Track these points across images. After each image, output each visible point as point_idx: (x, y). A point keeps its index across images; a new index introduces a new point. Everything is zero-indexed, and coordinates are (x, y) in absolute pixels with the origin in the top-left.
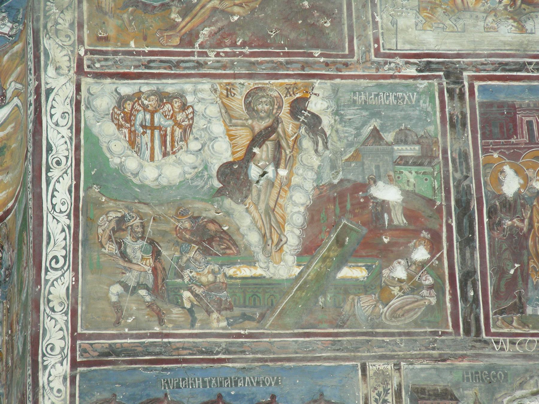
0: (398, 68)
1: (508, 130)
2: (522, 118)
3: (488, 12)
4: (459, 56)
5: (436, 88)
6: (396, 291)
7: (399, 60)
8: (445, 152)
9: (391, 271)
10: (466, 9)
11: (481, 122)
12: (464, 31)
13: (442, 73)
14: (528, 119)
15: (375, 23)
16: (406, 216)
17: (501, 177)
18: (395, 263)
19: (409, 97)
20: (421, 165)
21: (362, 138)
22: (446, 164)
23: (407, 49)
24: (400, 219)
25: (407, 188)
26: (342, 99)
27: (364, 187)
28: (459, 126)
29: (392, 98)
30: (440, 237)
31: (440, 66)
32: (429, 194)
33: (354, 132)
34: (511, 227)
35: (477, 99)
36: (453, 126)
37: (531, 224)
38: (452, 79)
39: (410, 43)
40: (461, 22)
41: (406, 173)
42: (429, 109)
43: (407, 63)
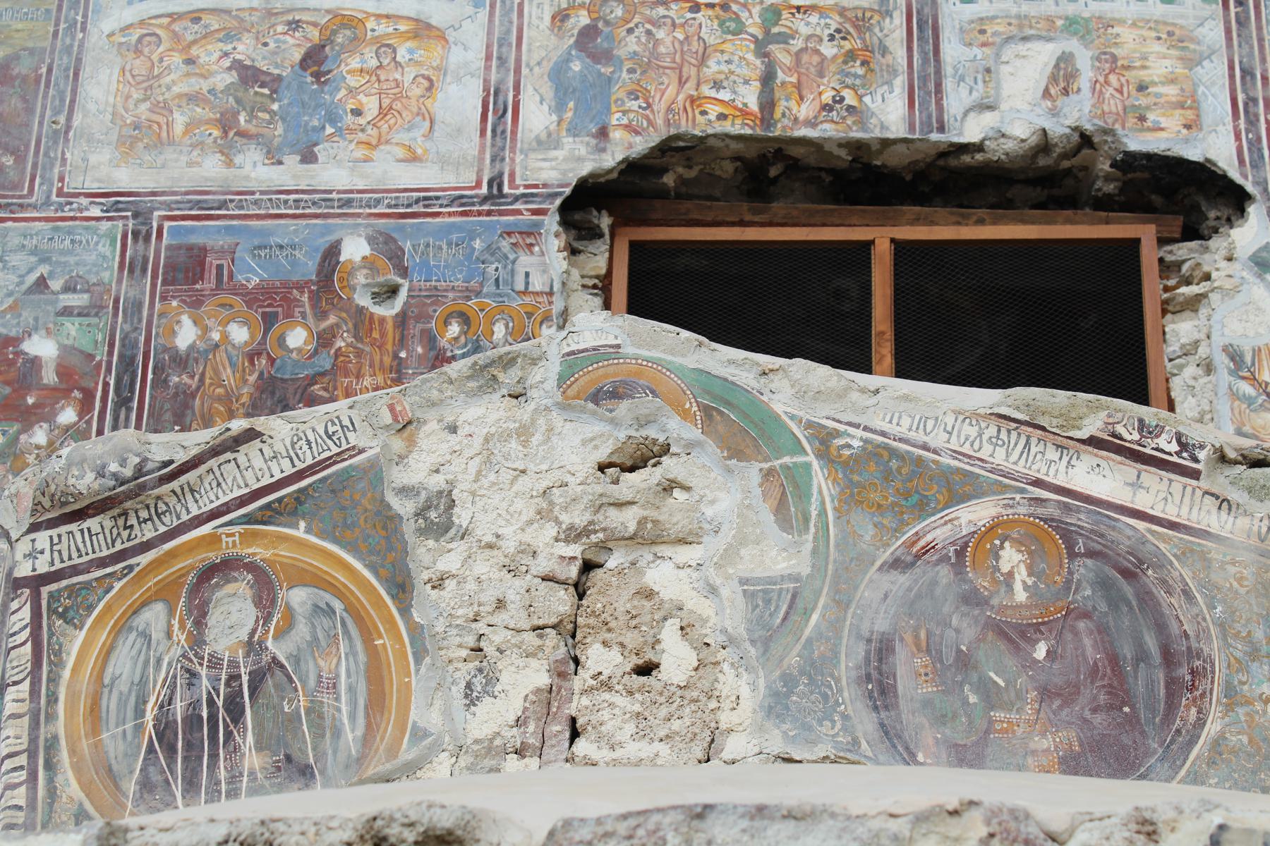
0: (81, 211)
1: (194, 275)
2: (212, 261)
3: (193, 146)
4: (154, 194)
5: (120, 230)
6: (31, 459)
7: (84, 201)
8: (117, 301)
9: (30, 437)
10: (171, 142)
11: (165, 266)
12: (163, 167)
13: (129, 214)
14: (219, 262)
15: (64, 160)
16: (58, 374)
17: (176, 328)
18: (36, 428)
19: (87, 241)
20: (87, 315)
21: (24, 287)
22: (116, 314)
23: (94, 187)
24: (49, 376)
25: (66, 342)
26: (10, 244)
27: (16, 341)
28: (138, 272)
29: (67, 242)
30: (94, 397)
31: (130, 206)
32: (89, 349)
33: (17, 280)
34: (177, 386)
35: (165, 241)
36: (131, 271)
37: (202, 380)
38: (140, 220)
39: (99, 181)
40: (162, 157)
41: (68, 325)
42: (108, 254)
43: (91, 203)
